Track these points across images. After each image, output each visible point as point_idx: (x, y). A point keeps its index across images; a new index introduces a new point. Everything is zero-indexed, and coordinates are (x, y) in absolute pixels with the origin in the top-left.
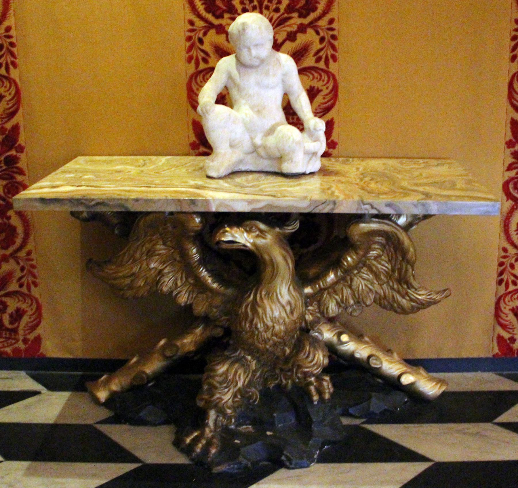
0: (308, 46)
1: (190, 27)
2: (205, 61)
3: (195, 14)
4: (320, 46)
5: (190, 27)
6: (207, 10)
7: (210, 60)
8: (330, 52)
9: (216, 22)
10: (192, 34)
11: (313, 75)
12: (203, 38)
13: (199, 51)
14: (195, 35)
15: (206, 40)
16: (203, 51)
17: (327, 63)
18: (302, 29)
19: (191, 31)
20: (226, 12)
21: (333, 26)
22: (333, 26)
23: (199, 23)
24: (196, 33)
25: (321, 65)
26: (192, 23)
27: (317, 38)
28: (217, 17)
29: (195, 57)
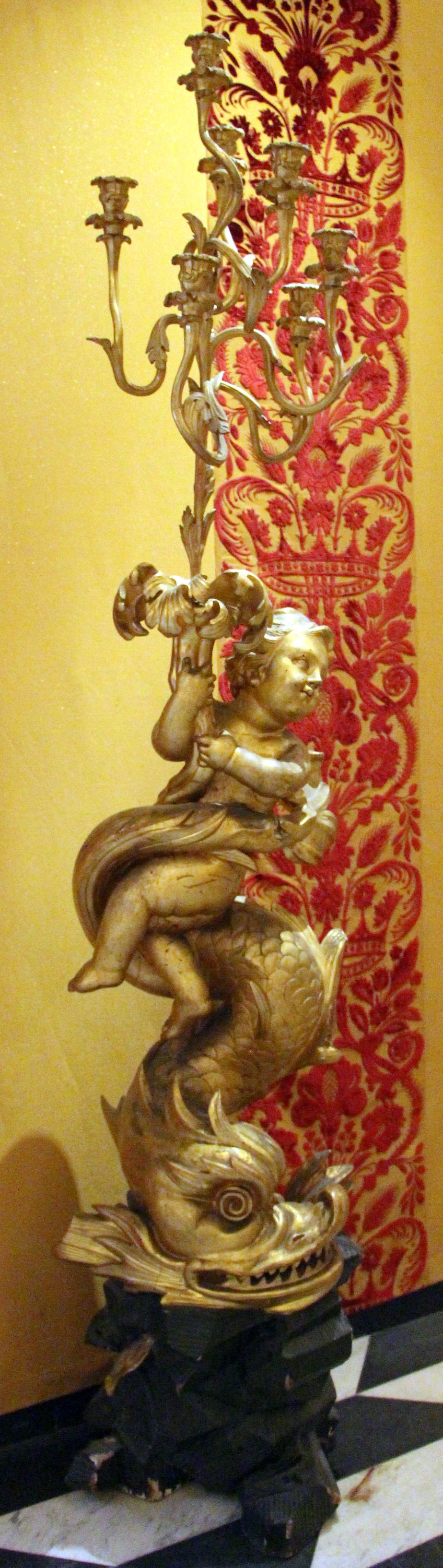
0: (375, 455)
2: (242, 467)
4: (392, 456)
8: (403, 466)
11: (383, 498)
13: (233, 449)
16: (236, 448)
17: (400, 484)
18: (369, 427)
21: (405, 426)
22: (405, 426)
25: (393, 485)
27: (387, 443)
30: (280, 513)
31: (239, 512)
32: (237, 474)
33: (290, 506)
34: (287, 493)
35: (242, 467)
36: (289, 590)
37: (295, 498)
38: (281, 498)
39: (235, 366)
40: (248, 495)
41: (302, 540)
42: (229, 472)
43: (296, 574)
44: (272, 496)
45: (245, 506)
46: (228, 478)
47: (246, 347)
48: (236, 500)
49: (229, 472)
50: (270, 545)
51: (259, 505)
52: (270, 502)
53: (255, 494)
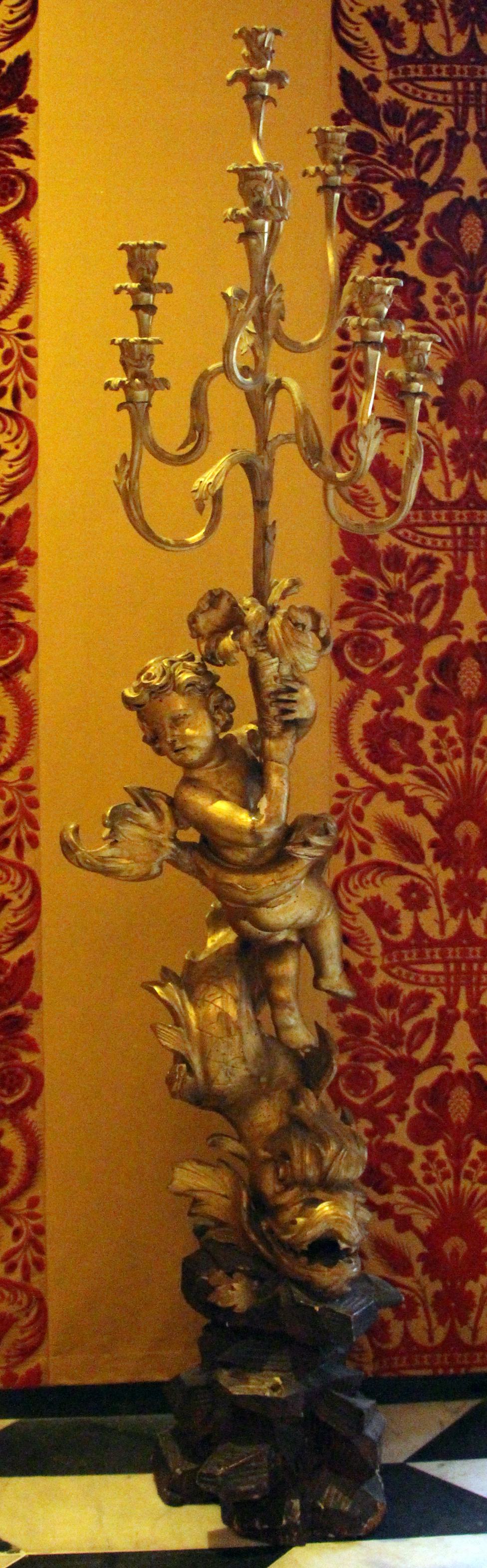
1: (340, 788)
2: (366, 850)
3: (350, 765)
5: (340, 788)
6: (374, 758)
7: (373, 847)
9: (388, 779)
10: (343, 801)
12: (363, 807)
14: (349, 801)
15: (368, 811)
19: (340, 795)
20: (408, 762)
23: (357, 782)
24: (351, 799)
26: (342, 780)
28: (390, 771)
29: (346, 842)
30: (414, 895)
31: (360, 900)
32: (360, 859)
33: (428, 888)
34: (425, 874)
35: (366, 850)
36: (422, 979)
37: (435, 880)
38: (417, 880)
39: (361, 740)
40: (373, 881)
41: (442, 924)
42: (350, 856)
43: (434, 962)
44: (407, 879)
45: (367, 893)
46: (347, 864)
47: (377, 717)
48: (356, 887)
49: (350, 856)
50: (400, 933)
51: (389, 890)
52: (402, 886)
53: (382, 880)
